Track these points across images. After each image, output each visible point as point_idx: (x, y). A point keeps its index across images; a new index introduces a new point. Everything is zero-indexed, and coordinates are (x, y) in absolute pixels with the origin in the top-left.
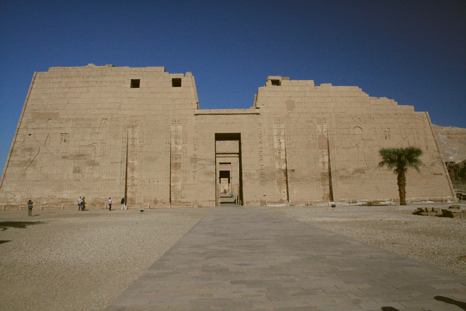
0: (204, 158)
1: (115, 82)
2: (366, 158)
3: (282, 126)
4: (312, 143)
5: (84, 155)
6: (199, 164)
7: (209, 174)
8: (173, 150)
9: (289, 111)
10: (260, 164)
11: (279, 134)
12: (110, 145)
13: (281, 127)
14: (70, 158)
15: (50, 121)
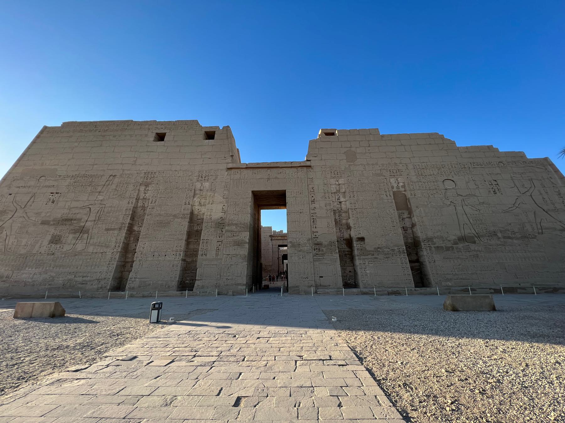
0: (234, 222)
1: (136, 135)
2: (471, 221)
3: (341, 181)
4: (386, 201)
5: (72, 220)
6: (227, 231)
7: (239, 244)
8: (196, 213)
9: (349, 163)
10: (313, 229)
11: (338, 191)
12: (111, 207)
13: (340, 182)
14: (52, 223)
15: (42, 178)
